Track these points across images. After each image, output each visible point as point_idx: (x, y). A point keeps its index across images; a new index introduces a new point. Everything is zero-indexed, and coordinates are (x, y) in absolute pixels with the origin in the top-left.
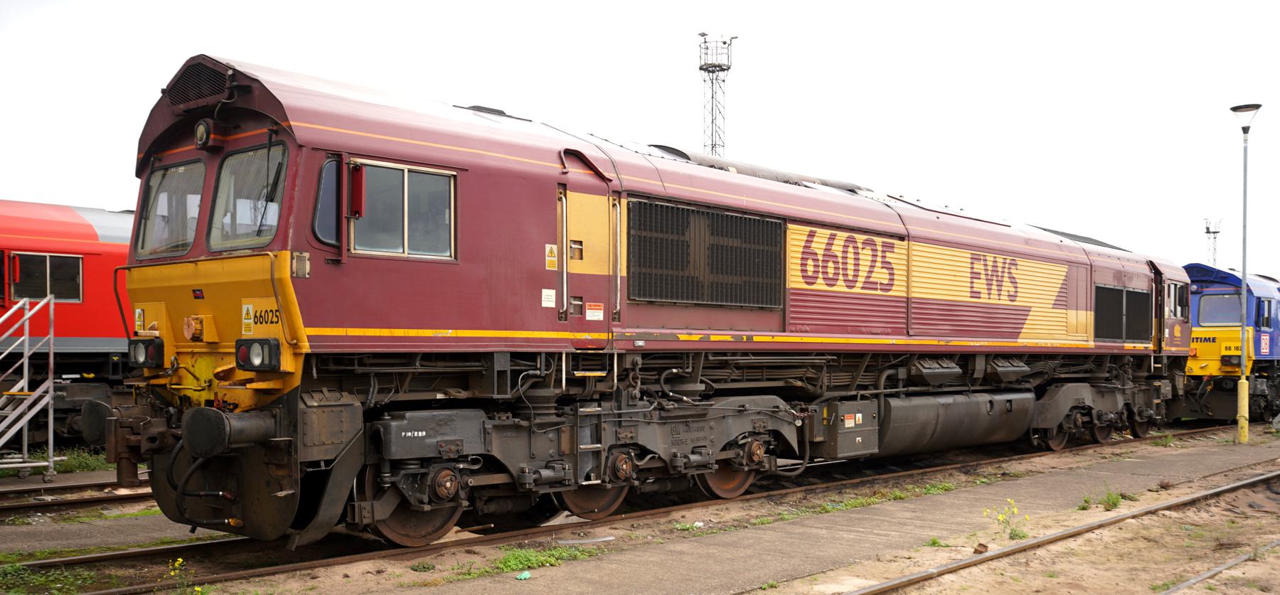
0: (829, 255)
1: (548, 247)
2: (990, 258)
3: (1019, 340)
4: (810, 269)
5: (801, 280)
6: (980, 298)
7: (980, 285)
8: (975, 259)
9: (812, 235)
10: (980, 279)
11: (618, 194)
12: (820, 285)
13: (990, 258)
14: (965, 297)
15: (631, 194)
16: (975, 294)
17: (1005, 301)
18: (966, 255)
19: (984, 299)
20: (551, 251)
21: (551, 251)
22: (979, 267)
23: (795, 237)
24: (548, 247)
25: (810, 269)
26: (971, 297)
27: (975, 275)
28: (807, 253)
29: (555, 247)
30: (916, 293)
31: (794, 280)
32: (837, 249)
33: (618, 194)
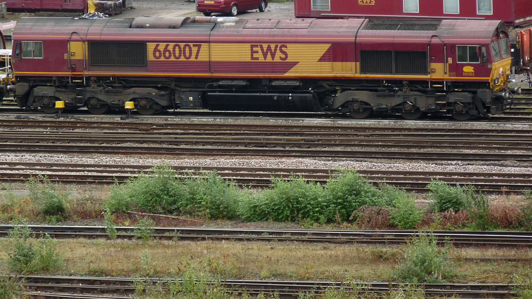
0: (166, 50)
1: (65, 54)
2: (265, 46)
3: (286, 74)
4: (157, 54)
5: (154, 58)
6: (258, 59)
7: (260, 56)
8: (252, 47)
9: (158, 45)
10: (258, 53)
11: (84, 41)
12: (162, 59)
14: (248, 59)
15: (88, 41)
16: (252, 58)
17: (277, 59)
18: (249, 45)
19: (262, 59)
20: (66, 55)
21: (66, 55)
22: (258, 49)
23: (151, 47)
24: (65, 54)
25: (157, 54)
26: (251, 59)
27: (253, 52)
28: (156, 50)
29: (67, 54)
30: (214, 59)
31: (150, 57)
32: (170, 48)
33: (84, 41)
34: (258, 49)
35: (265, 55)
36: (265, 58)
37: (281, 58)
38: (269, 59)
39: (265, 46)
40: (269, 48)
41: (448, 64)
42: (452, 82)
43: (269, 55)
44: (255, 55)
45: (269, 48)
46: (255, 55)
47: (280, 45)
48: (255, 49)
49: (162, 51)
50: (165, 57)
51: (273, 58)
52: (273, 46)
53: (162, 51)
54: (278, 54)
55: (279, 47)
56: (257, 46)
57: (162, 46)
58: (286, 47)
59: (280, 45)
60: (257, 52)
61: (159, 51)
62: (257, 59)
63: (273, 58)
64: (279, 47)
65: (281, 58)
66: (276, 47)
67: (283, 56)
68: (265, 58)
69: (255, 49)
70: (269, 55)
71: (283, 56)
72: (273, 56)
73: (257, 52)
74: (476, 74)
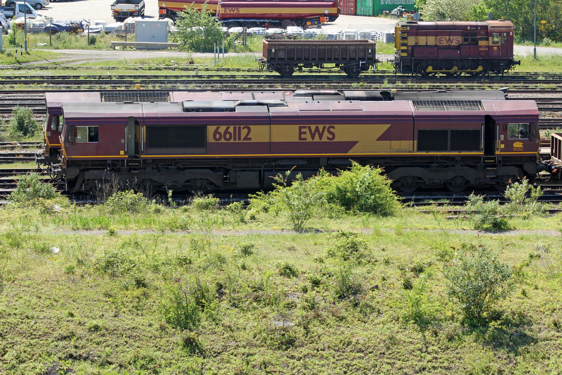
0: (226, 132)
4: (218, 136)
8: (300, 128)
12: (223, 140)
13: (313, 127)
14: (296, 139)
16: (300, 138)
17: (324, 139)
18: (297, 127)
19: (309, 139)
25: (218, 136)
27: (301, 133)
28: (216, 132)
34: (307, 130)
35: (313, 136)
36: (313, 138)
37: (328, 138)
38: (317, 139)
39: (313, 127)
40: (317, 129)
41: (500, 141)
42: (503, 157)
43: (317, 134)
44: (303, 136)
45: (317, 129)
46: (303, 136)
47: (328, 126)
48: (303, 130)
49: (223, 134)
50: (225, 139)
51: (321, 139)
53: (223, 134)
54: (326, 135)
55: (327, 128)
56: (305, 127)
57: (222, 129)
58: (334, 128)
59: (328, 126)
60: (305, 133)
61: (220, 133)
62: (305, 139)
63: (321, 139)
64: (327, 128)
65: (328, 138)
66: (324, 128)
67: (331, 136)
68: (313, 138)
69: (303, 130)
70: (317, 134)
71: (331, 136)
72: (321, 136)
73: (305, 133)
74: (525, 149)
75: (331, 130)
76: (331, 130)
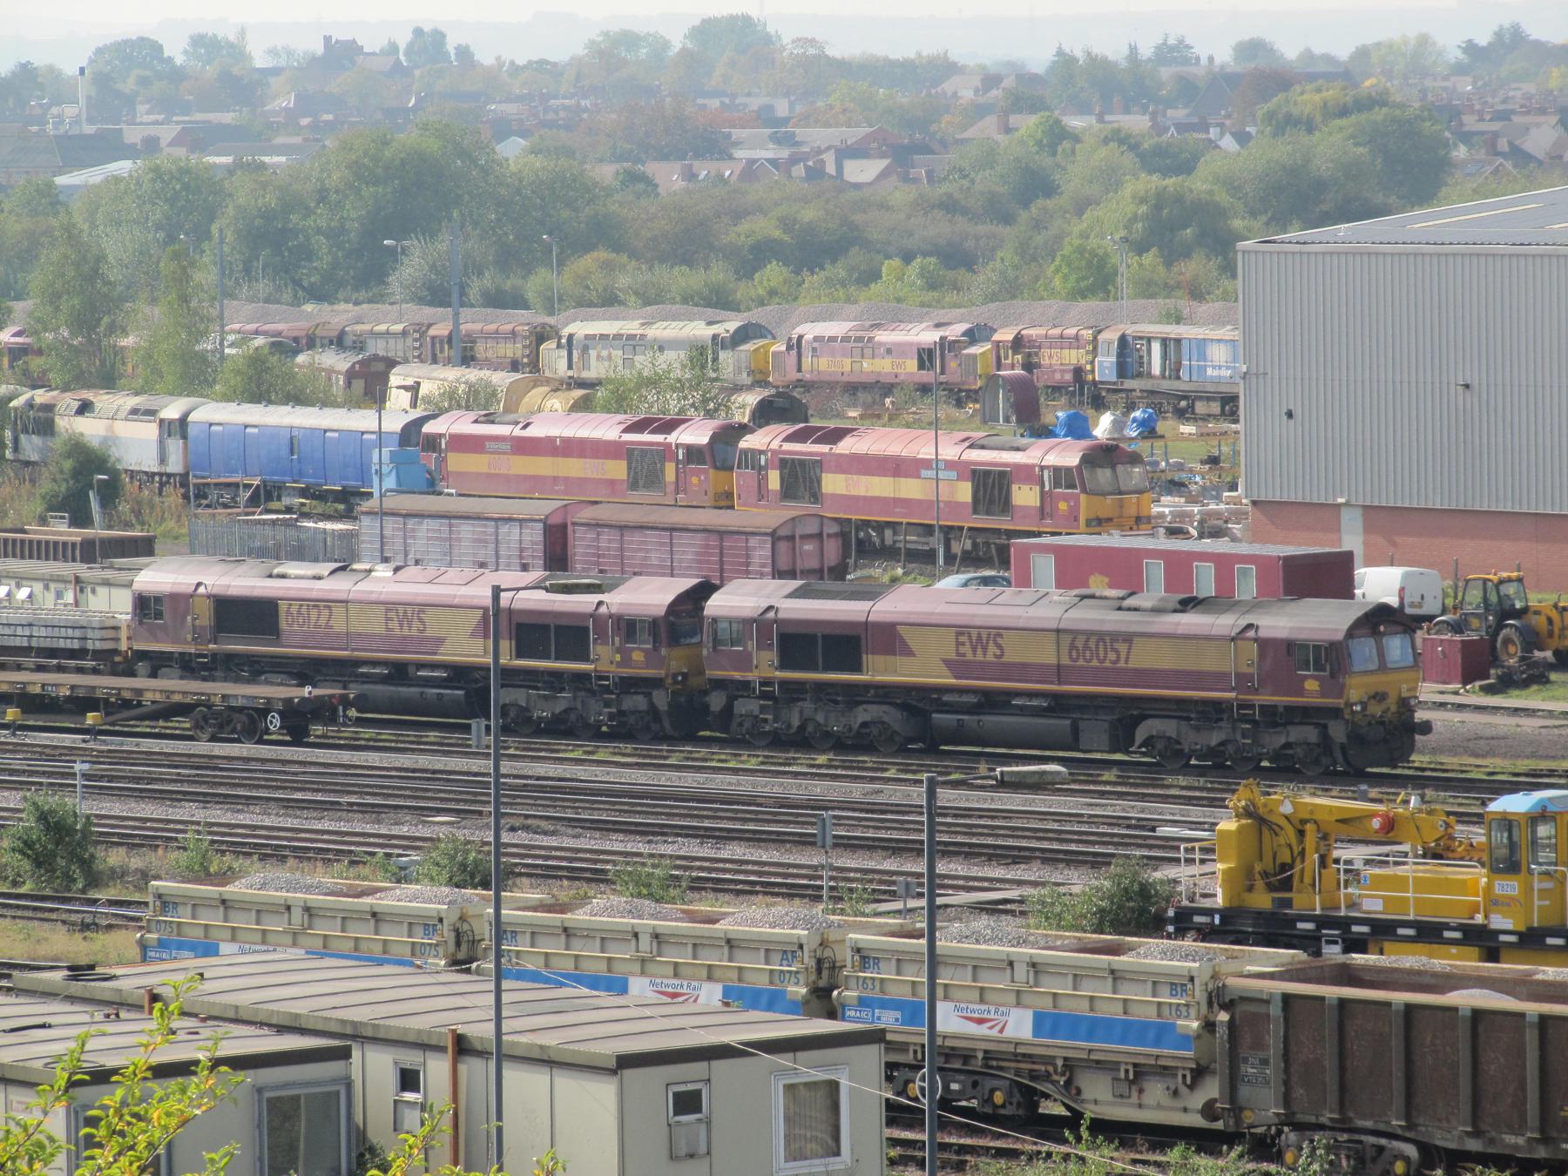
7: (967, 649)
16: (958, 654)
19: (970, 656)
35: (974, 650)
36: (975, 655)
37: (996, 656)
38: (980, 657)
39: (974, 632)
40: (979, 637)
43: (979, 651)
45: (979, 637)
46: (961, 648)
48: (962, 639)
51: (985, 655)
52: (984, 633)
54: (992, 649)
56: (962, 634)
58: (1000, 635)
60: (963, 644)
62: (964, 655)
63: (985, 655)
65: (996, 656)
67: (998, 652)
68: (975, 655)
69: (962, 639)
70: (979, 651)
71: (998, 652)
73: (963, 644)
75: (999, 640)
76: (999, 640)
